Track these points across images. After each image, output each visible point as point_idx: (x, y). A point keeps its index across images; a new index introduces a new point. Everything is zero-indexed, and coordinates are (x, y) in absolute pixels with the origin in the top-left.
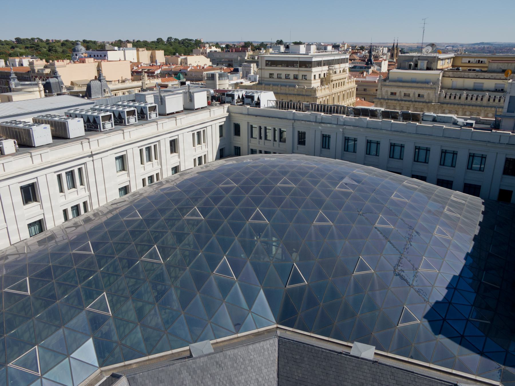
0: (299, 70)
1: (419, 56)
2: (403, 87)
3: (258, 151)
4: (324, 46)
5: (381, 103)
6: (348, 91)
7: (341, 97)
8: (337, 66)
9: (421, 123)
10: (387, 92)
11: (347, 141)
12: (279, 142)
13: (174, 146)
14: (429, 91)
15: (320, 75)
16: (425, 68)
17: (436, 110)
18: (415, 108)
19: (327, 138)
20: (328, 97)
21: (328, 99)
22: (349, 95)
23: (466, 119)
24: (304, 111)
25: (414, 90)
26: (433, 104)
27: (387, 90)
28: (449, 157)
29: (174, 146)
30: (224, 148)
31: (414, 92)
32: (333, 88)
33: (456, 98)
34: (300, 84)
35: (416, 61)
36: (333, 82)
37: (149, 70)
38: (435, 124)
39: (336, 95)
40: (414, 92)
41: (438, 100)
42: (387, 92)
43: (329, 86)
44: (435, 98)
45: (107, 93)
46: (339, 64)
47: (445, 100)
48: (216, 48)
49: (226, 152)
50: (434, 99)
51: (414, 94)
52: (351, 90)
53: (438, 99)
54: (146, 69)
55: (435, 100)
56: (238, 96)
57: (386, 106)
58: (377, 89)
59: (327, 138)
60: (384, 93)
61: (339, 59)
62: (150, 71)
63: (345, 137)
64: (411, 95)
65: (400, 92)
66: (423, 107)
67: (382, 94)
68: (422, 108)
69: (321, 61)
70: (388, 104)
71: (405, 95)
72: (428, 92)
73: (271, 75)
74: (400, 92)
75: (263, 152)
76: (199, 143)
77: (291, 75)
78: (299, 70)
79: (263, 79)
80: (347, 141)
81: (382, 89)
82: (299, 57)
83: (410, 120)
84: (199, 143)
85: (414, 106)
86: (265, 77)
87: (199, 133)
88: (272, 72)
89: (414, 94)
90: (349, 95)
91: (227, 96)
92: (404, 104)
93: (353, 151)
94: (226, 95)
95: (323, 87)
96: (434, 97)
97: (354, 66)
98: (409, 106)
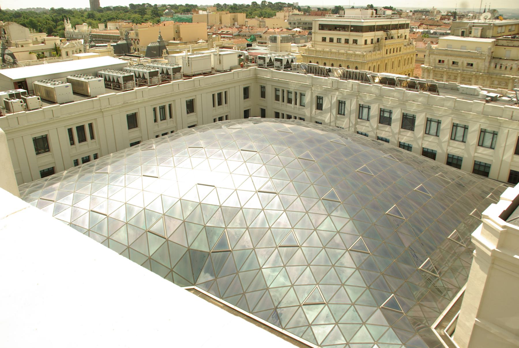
0: (349, 35)
1: (474, 23)
2: (451, 55)
3: (281, 115)
4: (383, 11)
5: (428, 71)
6: (405, 57)
7: (396, 63)
8: (393, 32)
9: (438, 95)
10: (435, 59)
11: (361, 108)
12: (294, 105)
13: (190, 106)
14: (479, 61)
15: (372, 40)
16: (479, 36)
17: (484, 80)
18: (463, 77)
19: (343, 104)
20: (379, 63)
21: (379, 65)
22: (406, 62)
23: (489, 92)
24: (325, 77)
25: (462, 58)
26: (481, 74)
27: (435, 58)
28: (460, 131)
29: (190, 106)
30: (250, 109)
31: (463, 61)
32: (387, 53)
33: (507, 68)
34: (351, 49)
35: (470, 28)
36: (386, 48)
37: (227, 32)
38: (447, 95)
39: (390, 60)
40: (463, 61)
41: (488, 70)
42: (435, 59)
43: (382, 52)
44: (485, 68)
45: (165, 54)
46: (397, 29)
47: (494, 71)
48: (299, 11)
50: (484, 69)
51: (463, 63)
52: (409, 57)
53: (487, 69)
54: (224, 32)
55: (484, 70)
56: (269, 59)
57: (433, 74)
58: (425, 54)
59: (343, 104)
60: (432, 61)
61: (398, 24)
62: (228, 33)
63: (360, 104)
64: (460, 64)
65: (448, 61)
66: (471, 77)
67: (429, 62)
68: (470, 78)
69: (375, 25)
70: (436, 72)
71: (454, 63)
72: (477, 61)
73: (324, 39)
74: (448, 61)
76: (220, 103)
77: (342, 39)
78: (349, 35)
79: (316, 43)
80: (361, 108)
81: (430, 56)
82: (350, 22)
83: (427, 90)
84: (220, 103)
85: (462, 75)
86: (318, 40)
87: (220, 95)
88: (324, 36)
89: (463, 63)
90: (406, 62)
91: (259, 59)
92: (452, 73)
93: (367, 119)
94: (258, 58)
95: (374, 53)
96: (483, 67)
97: (434, 32)
98: (456, 75)
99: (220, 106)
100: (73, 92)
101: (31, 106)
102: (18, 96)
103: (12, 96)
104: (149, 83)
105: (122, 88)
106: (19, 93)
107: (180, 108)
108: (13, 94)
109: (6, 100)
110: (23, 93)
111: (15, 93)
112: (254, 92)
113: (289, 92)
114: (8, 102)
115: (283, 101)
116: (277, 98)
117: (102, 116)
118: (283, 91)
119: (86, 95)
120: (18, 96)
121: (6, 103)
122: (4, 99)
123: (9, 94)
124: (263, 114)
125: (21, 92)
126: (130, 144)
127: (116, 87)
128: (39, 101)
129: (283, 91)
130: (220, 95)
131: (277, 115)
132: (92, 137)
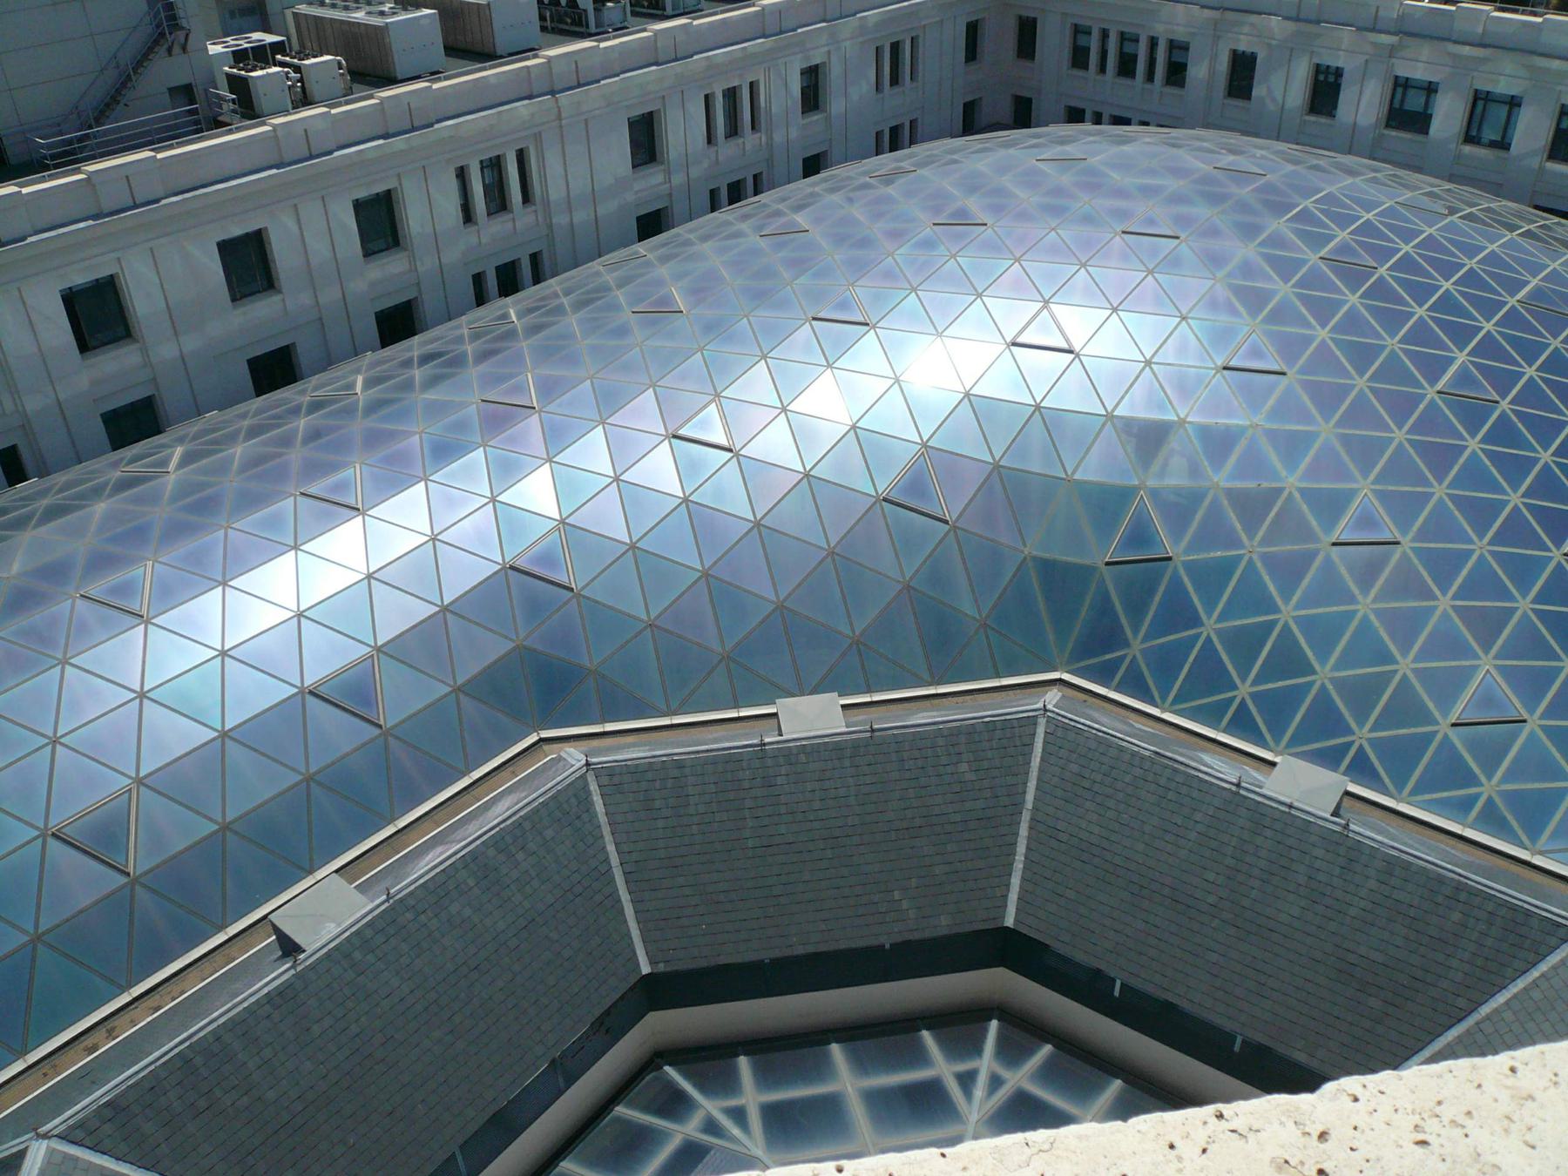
3: (1088, 115)
49: (985, 114)
75: (1105, 118)
76: (895, 80)
84: (895, 80)
99: (896, 90)
100: (445, 48)
101: (315, 89)
102: (262, 55)
103: (239, 57)
104: (669, 11)
105: (587, 26)
106: (265, 45)
107: (780, 95)
108: (246, 49)
109: (235, 70)
110: (278, 48)
111: (252, 48)
112: (1000, 41)
113: (1123, 37)
114: (244, 80)
115: (1102, 68)
116: (1079, 58)
117: (556, 123)
118: (1105, 34)
119: (486, 55)
120: (262, 55)
121: (240, 86)
122: (227, 68)
123: (233, 52)
124: (1023, 115)
125: (270, 44)
126: (639, 219)
127: (561, 21)
128: (342, 75)
129: (1105, 34)
130: (896, 48)
131: (1075, 115)
132: (527, 198)
